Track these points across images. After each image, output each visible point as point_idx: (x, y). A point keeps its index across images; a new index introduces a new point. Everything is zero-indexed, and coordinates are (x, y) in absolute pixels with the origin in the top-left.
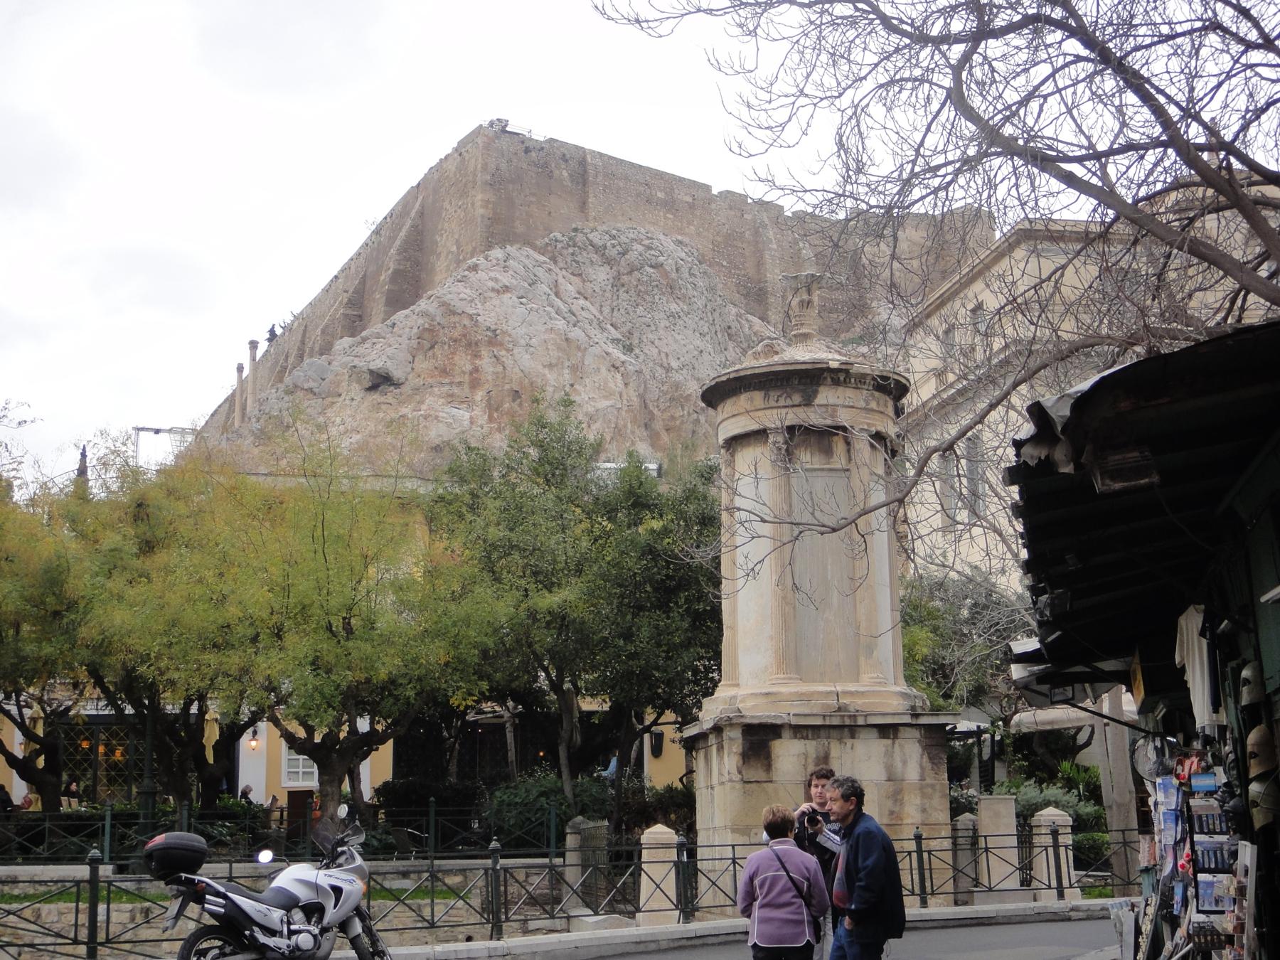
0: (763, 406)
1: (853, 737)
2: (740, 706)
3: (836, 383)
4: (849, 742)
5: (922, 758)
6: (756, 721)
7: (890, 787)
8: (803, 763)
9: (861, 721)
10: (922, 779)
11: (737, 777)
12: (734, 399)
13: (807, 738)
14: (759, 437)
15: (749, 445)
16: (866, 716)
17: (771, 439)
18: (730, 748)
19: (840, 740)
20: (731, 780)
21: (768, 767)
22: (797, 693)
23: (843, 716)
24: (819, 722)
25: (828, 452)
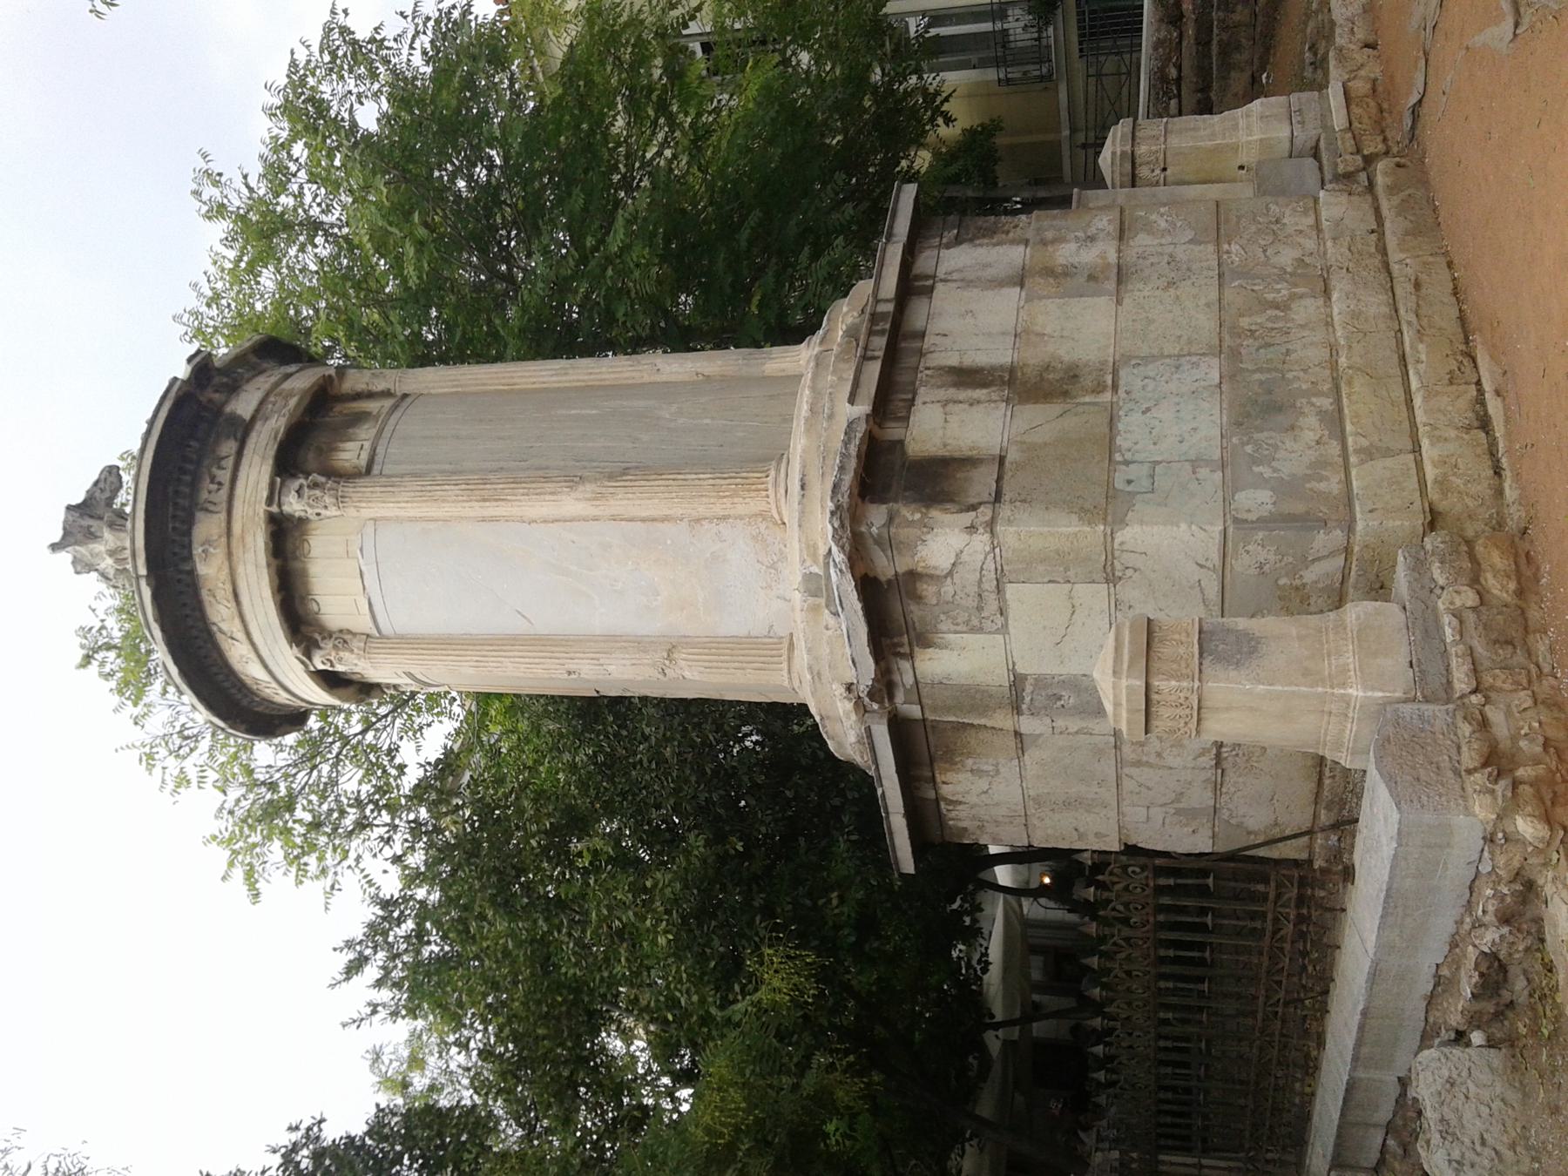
0: (223, 516)
1: (922, 335)
2: (822, 551)
3: (233, 389)
4: (929, 341)
5: (981, 245)
6: (852, 464)
7: (1037, 283)
8: (966, 406)
9: (890, 307)
10: (1026, 243)
11: (985, 513)
12: (204, 593)
13: (912, 402)
14: (289, 546)
15: (304, 574)
16: (877, 301)
17: (293, 505)
18: (911, 524)
19: (921, 353)
20: (991, 525)
21: (969, 462)
22: (807, 420)
23: (871, 333)
24: (874, 370)
25: (360, 418)
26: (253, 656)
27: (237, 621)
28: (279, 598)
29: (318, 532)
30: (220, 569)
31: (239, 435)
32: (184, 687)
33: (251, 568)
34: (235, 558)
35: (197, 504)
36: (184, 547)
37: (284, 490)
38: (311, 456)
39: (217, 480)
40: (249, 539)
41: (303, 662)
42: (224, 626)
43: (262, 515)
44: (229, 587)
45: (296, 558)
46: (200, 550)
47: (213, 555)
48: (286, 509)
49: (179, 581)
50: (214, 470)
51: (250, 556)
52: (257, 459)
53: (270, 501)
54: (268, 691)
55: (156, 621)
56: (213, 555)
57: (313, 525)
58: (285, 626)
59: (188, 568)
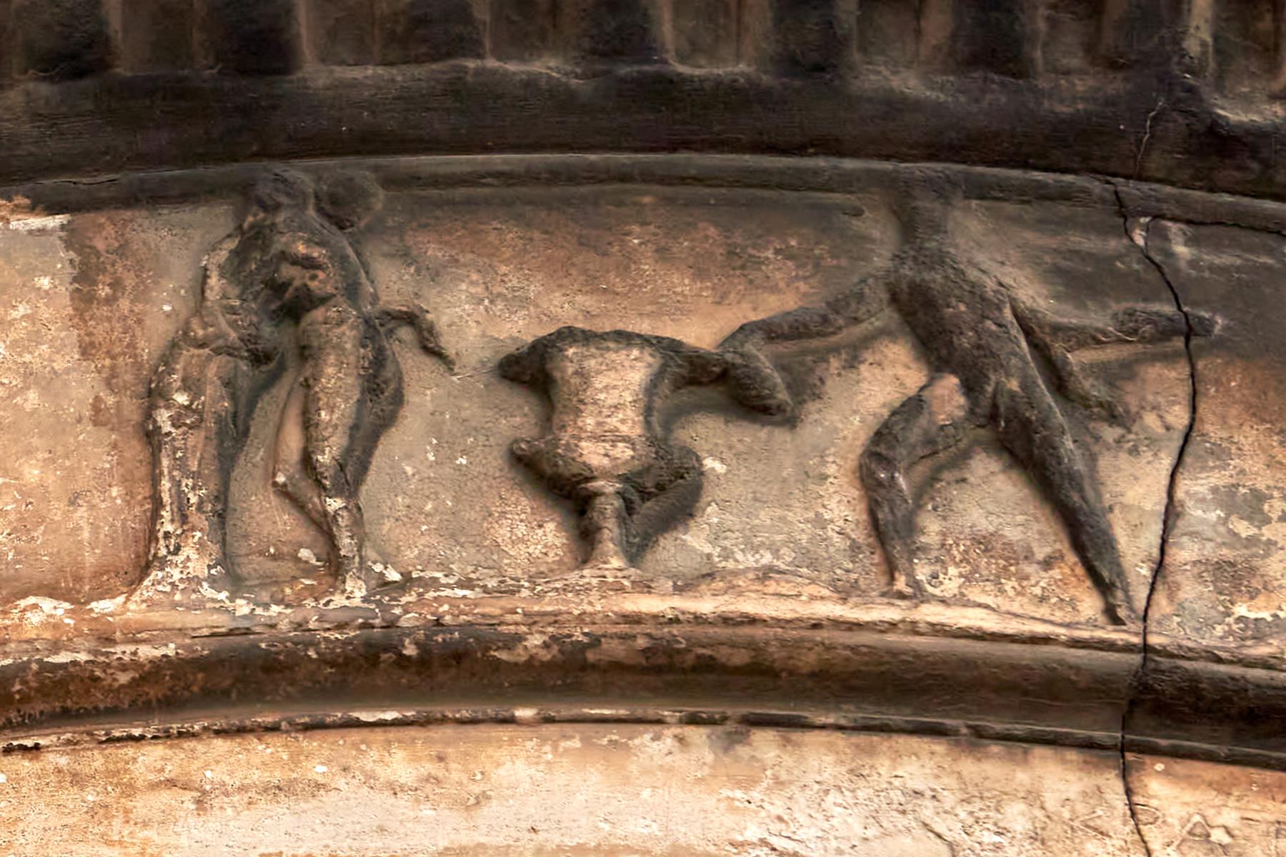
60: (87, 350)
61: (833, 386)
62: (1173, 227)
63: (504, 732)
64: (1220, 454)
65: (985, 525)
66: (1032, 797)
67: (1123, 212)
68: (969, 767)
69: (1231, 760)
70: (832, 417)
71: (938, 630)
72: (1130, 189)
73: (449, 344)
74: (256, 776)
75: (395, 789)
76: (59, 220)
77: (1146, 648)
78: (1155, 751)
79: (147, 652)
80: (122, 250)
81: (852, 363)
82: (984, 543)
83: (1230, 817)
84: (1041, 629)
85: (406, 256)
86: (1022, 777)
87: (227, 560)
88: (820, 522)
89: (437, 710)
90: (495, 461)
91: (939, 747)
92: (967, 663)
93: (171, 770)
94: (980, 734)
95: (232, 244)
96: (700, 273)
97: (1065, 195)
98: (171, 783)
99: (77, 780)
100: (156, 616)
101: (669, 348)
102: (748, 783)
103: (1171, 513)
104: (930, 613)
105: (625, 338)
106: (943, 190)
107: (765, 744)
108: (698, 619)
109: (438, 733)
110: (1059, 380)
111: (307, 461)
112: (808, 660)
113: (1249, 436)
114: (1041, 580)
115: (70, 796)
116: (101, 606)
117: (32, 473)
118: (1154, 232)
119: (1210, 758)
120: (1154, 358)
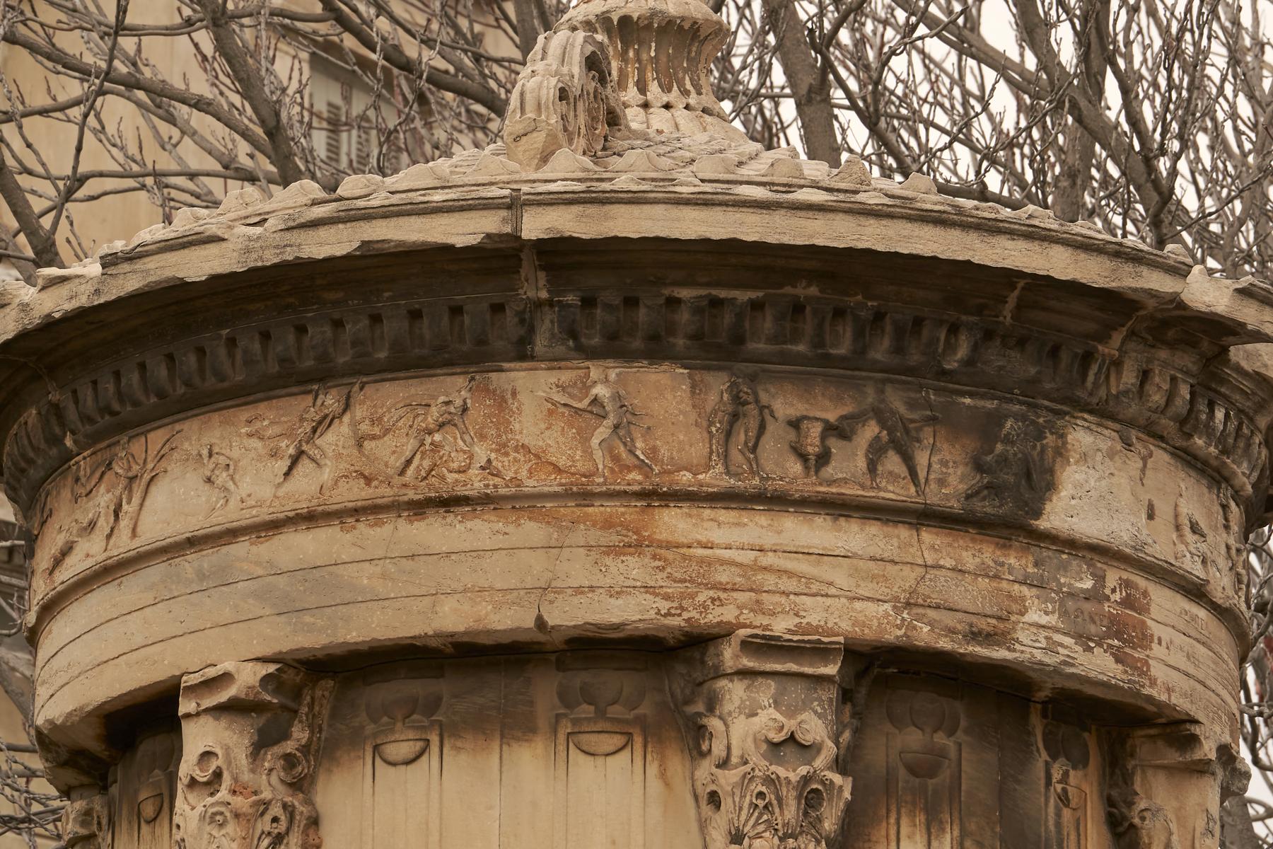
0: (715, 479)
26: (232, 515)
27: (354, 493)
28: (433, 643)
29: (655, 785)
30: (539, 459)
31: (986, 507)
32: (130, 282)
33: (537, 567)
34: (570, 510)
35: (753, 379)
36: (612, 337)
37: (796, 691)
38: (913, 739)
39: (835, 445)
40: (635, 568)
41: (210, 684)
42: (336, 438)
43: (715, 616)
44: (476, 484)
45: (567, 701)
46: (601, 391)
47: (584, 438)
48: (734, 693)
49: (498, 309)
50: (870, 430)
51: (577, 569)
52: (905, 578)
53: (766, 646)
54: (103, 499)
55: (365, 244)
56: (584, 438)
57: (677, 764)
58: (338, 651)
59: (540, 344)
60: (694, 406)
61: (859, 431)
62: (931, 391)
63: (786, 514)
64: (940, 450)
65: (891, 469)
66: (898, 537)
67: (921, 387)
68: (885, 528)
69: (940, 527)
70: (859, 440)
71: (883, 498)
72: (922, 381)
73: (776, 415)
74: (731, 520)
75: (762, 527)
76: (686, 371)
77: (926, 504)
78: (923, 525)
79: (710, 490)
80: (702, 381)
81: (863, 426)
82: (891, 473)
83: (938, 542)
84: (904, 499)
85: (767, 391)
86: (896, 531)
87: (727, 467)
88: (856, 467)
89: (771, 507)
90: (787, 447)
91: (879, 523)
92: (889, 506)
93: (712, 516)
94: (888, 520)
95: (728, 384)
96: (831, 400)
97: (908, 383)
98: (712, 520)
99: (690, 516)
100: (713, 482)
101: (826, 422)
102: (840, 531)
103: (930, 466)
104: (882, 494)
105: (817, 419)
106: (884, 381)
107: (842, 521)
108: (832, 493)
109: (773, 513)
110: (907, 431)
111: (746, 443)
112: (854, 503)
113: (945, 446)
114: (902, 483)
115: (689, 520)
116: (700, 477)
117: (682, 437)
118: (927, 393)
119: (935, 527)
120: (925, 426)
